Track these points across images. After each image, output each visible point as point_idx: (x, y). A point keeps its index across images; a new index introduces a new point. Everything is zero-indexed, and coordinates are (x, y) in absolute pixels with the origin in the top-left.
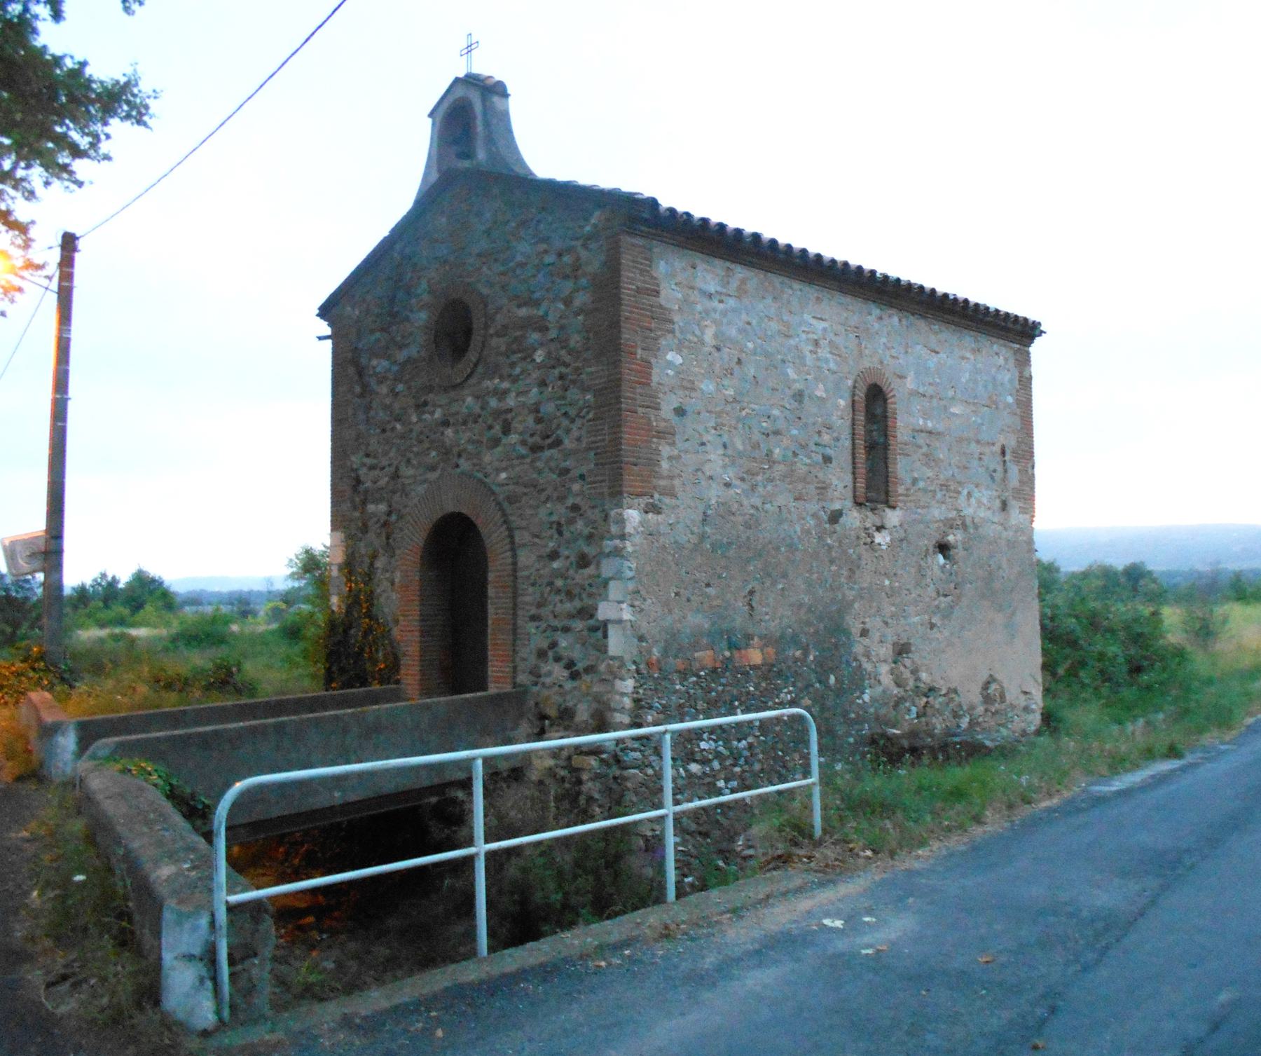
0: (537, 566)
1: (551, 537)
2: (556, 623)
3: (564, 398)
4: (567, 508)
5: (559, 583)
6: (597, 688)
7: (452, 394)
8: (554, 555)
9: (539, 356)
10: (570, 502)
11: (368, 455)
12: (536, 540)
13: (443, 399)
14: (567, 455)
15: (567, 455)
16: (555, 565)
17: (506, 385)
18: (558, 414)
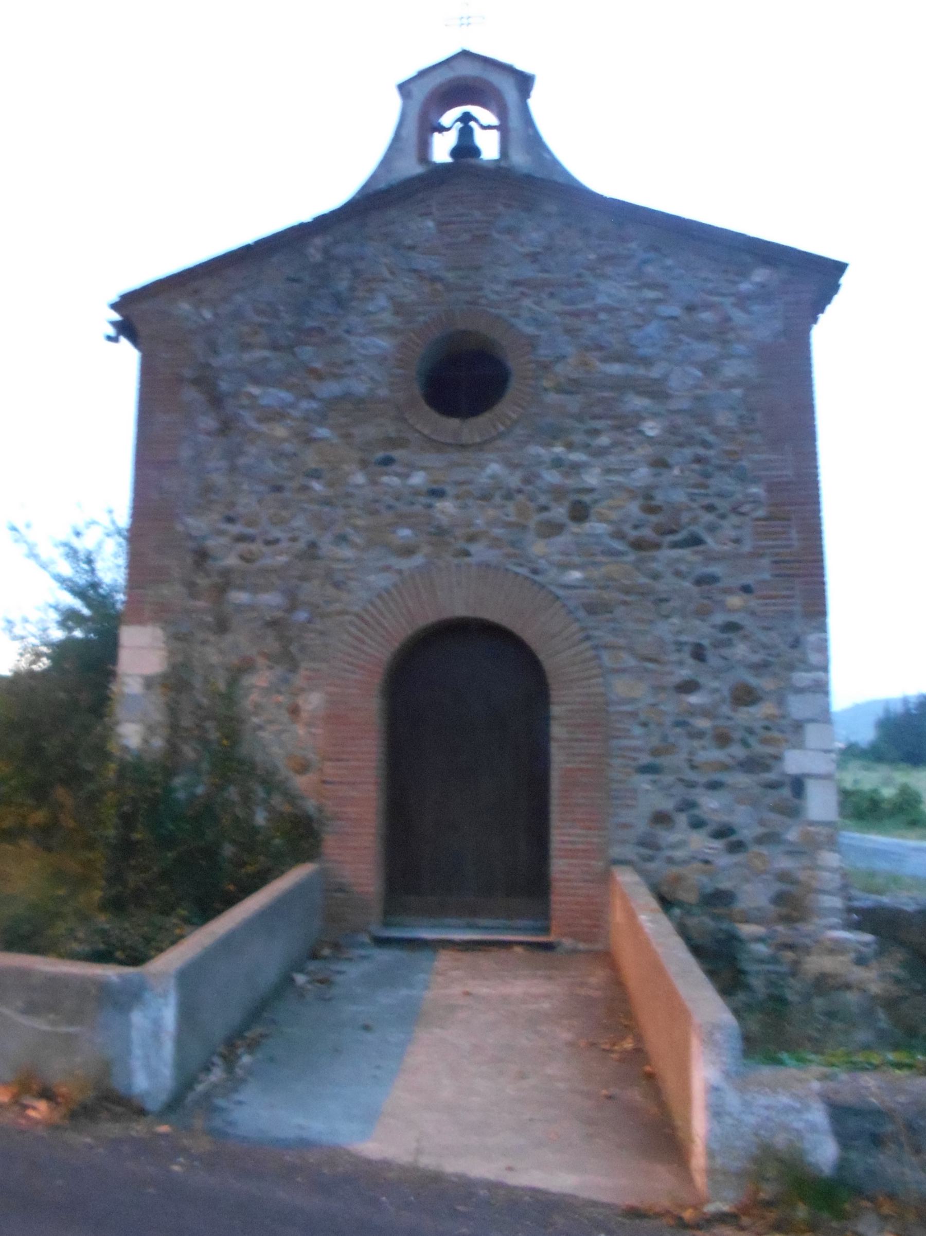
0: (651, 700)
1: (681, 663)
2: (691, 776)
3: (706, 487)
4: (714, 626)
5: (703, 723)
6: (785, 864)
7: (456, 456)
8: (689, 687)
9: (651, 428)
10: (719, 618)
11: (230, 520)
12: (650, 665)
13: (432, 459)
14: (711, 558)
15: (711, 558)
16: (694, 699)
17: (577, 456)
18: (694, 505)
